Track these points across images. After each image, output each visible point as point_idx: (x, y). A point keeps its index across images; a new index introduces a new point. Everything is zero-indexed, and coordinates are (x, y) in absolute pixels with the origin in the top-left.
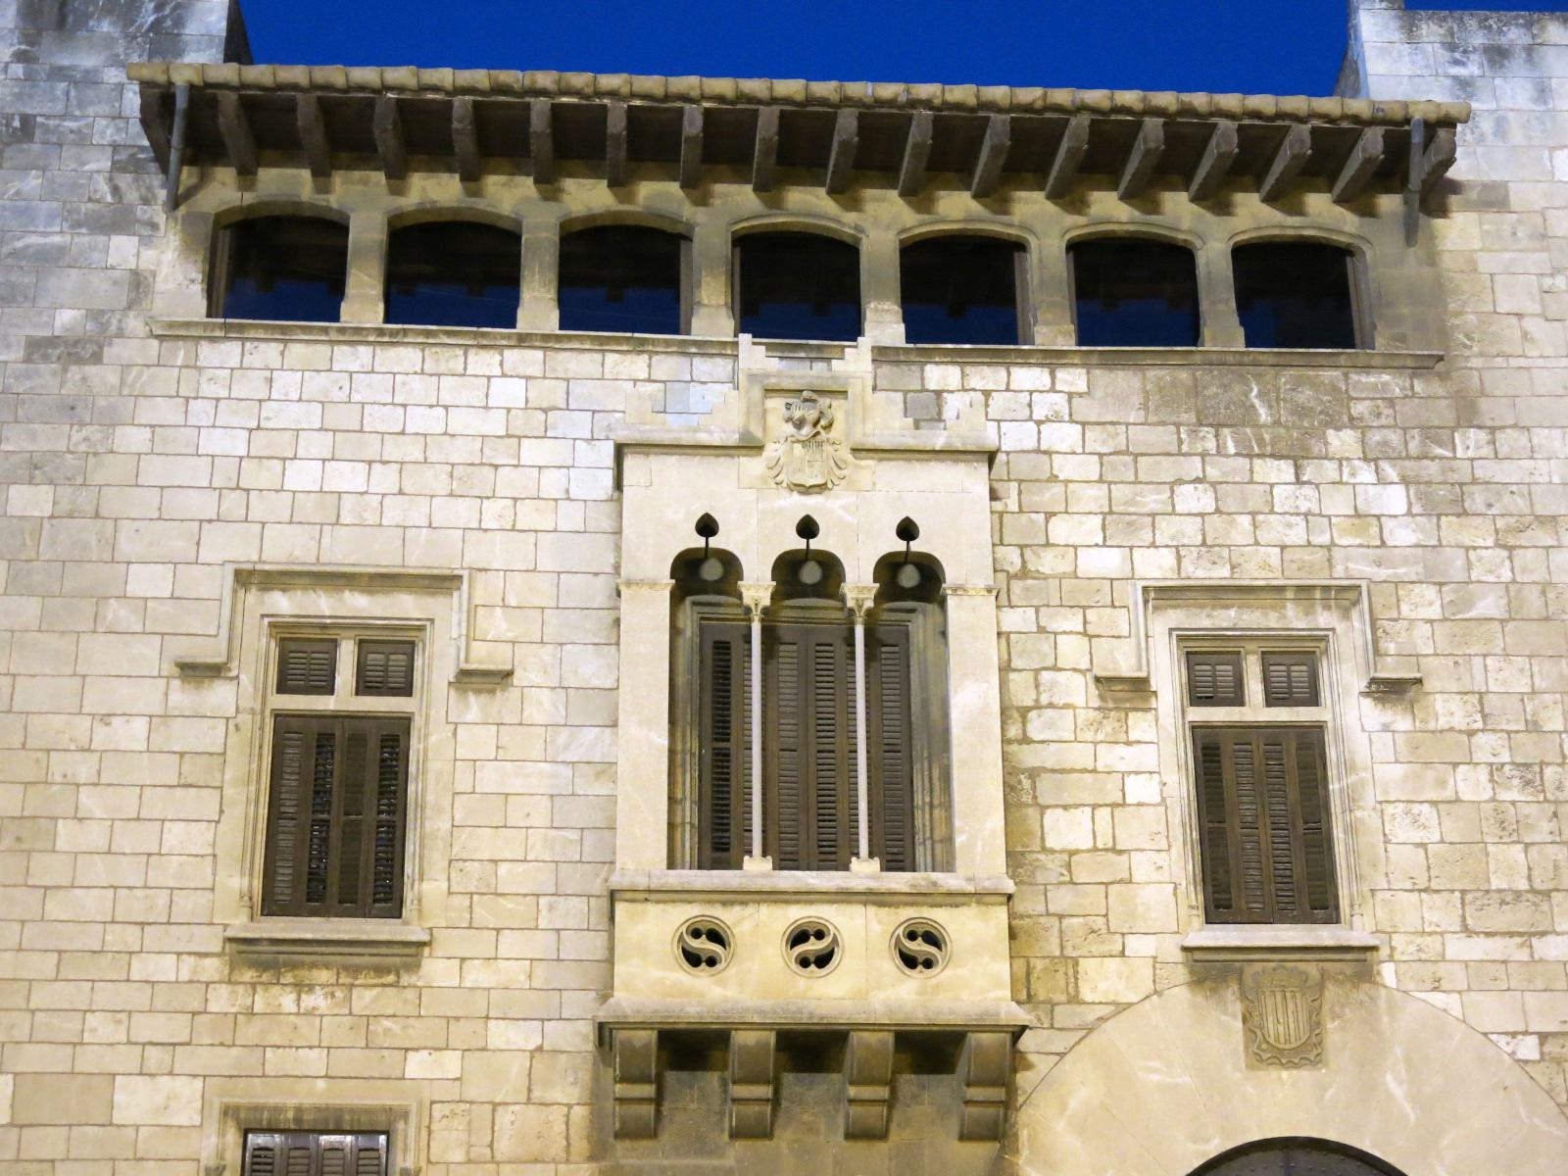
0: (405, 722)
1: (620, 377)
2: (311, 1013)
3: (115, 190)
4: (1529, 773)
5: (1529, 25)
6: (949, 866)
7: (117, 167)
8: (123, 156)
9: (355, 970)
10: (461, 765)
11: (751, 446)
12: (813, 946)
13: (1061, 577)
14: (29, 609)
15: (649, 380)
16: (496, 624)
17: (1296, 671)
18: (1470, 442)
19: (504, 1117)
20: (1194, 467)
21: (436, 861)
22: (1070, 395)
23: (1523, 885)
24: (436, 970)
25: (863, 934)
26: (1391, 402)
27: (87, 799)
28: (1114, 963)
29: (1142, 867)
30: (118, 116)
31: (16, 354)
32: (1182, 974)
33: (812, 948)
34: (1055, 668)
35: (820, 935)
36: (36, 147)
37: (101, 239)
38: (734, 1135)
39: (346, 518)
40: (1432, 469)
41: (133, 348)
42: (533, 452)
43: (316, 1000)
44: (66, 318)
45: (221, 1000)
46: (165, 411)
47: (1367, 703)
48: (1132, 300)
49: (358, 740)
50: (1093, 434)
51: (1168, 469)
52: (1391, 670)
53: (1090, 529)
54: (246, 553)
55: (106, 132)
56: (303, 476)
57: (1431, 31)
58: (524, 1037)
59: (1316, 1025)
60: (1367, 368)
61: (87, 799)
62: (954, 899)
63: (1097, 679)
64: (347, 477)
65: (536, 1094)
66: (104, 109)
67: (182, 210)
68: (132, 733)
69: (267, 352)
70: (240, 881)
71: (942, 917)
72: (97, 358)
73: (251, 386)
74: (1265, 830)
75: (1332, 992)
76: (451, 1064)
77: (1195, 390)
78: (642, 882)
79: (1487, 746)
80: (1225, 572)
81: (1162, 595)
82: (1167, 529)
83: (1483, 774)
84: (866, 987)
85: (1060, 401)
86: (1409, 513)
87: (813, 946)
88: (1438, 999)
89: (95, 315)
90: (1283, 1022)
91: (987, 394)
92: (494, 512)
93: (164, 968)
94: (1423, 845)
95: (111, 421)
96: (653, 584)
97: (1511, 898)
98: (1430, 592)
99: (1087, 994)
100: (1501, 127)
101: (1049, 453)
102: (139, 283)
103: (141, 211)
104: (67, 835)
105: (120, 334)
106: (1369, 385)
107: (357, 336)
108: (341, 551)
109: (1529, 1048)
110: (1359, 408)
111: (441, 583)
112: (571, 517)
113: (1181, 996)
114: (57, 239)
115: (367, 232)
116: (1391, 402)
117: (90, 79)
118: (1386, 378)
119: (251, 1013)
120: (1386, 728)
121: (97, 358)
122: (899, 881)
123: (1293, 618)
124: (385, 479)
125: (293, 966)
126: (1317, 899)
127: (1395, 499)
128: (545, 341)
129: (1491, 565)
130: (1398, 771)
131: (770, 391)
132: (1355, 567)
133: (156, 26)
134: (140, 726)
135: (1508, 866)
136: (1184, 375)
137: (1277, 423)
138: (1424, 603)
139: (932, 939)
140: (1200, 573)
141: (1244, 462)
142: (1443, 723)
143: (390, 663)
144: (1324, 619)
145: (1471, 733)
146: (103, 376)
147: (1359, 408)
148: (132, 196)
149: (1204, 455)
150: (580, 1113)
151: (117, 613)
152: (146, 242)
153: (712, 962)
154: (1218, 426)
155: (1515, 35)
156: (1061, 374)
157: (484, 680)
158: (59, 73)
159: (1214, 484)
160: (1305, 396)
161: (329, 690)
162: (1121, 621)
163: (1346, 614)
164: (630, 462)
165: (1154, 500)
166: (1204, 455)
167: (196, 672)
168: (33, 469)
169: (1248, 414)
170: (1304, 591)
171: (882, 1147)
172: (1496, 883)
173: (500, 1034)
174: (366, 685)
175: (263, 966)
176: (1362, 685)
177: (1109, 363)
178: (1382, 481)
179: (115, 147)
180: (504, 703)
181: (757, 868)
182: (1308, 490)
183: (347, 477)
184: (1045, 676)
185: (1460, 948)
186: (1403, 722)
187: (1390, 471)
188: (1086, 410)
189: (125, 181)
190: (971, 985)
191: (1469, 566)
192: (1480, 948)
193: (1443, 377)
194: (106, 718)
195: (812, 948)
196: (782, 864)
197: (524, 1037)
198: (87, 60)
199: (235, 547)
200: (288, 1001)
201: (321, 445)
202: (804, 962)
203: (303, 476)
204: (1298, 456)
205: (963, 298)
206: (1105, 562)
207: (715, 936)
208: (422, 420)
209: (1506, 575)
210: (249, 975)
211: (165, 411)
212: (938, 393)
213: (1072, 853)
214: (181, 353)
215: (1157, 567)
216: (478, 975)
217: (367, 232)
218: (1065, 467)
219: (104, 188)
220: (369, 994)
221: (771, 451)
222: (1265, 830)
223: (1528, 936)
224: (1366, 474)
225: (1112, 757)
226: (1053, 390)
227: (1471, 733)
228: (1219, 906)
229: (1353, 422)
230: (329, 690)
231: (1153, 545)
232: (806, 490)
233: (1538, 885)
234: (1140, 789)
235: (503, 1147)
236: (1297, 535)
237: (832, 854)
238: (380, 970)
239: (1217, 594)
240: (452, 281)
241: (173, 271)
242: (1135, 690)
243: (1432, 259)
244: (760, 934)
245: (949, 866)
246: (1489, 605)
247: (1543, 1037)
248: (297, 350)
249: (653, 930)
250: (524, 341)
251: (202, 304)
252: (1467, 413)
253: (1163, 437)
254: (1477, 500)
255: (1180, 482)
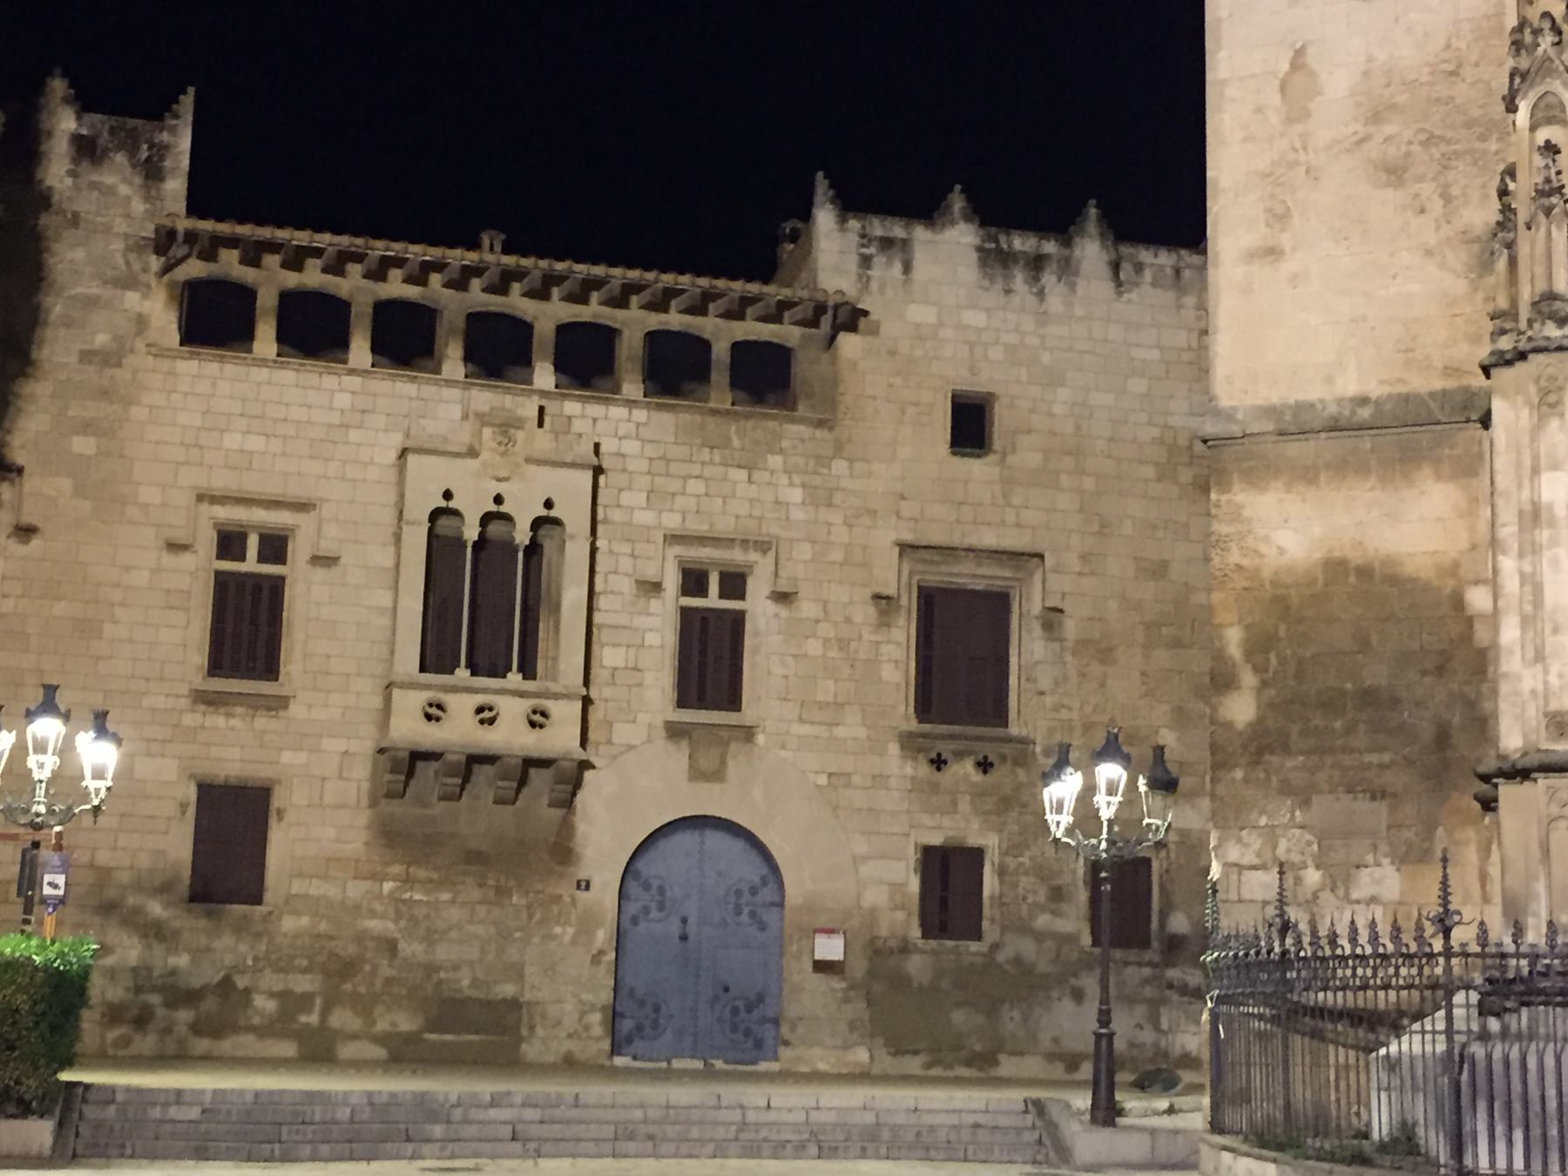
0: (282, 579)
1: (399, 391)
2: (233, 729)
3: (128, 263)
4: (843, 644)
5: (907, 226)
6: (555, 680)
7: (129, 249)
8: (131, 242)
9: (256, 708)
10: (308, 599)
11: (472, 453)
12: (487, 714)
13: (623, 524)
14: (86, 506)
15: (418, 398)
16: (331, 531)
17: (734, 584)
18: (840, 466)
19: (328, 785)
20: (696, 469)
21: (297, 654)
22: (638, 425)
23: (831, 699)
24: (295, 710)
25: (512, 710)
26: (803, 441)
27: (118, 611)
28: (629, 726)
29: (649, 678)
30: (128, 216)
31: (74, 359)
32: (663, 733)
33: (486, 715)
34: (615, 573)
35: (491, 709)
36: (80, 232)
37: (119, 292)
38: (442, 798)
39: (255, 465)
40: (817, 480)
41: (139, 359)
42: (355, 435)
43: (232, 722)
44: (101, 339)
45: (189, 719)
46: (158, 399)
47: (769, 602)
48: (674, 370)
49: (258, 588)
50: (648, 447)
51: (684, 469)
52: (783, 586)
53: (641, 498)
54: (202, 482)
55: (121, 226)
56: (232, 441)
57: (854, 224)
58: (339, 745)
59: (723, 763)
60: (793, 421)
61: (118, 611)
62: (557, 696)
63: (637, 581)
64: (256, 443)
65: (345, 774)
66: (120, 211)
67: (166, 278)
68: (140, 578)
69: (213, 368)
70: (199, 657)
71: (551, 706)
72: (119, 365)
73: (203, 387)
74: (710, 663)
75: (733, 747)
76: (302, 757)
77: (702, 427)
78: (407, 679)
79: (825, 629)
80: (705, 527)
81: (673, 539)
82: (680, 502)
83: (820, 642)
84: (510, 735)
85: (632, 426)
86: (803, 503)
87: (487, 714)
88: (783, 753)
89: (116, 338)
90: (707, 761)
91: (595, 420)
92: (333, 468)
93: (161, 702)
94: (786, 677)
95: (128, 402)
96: (419, 524)
97: (822, 706)
98: (807, 546)
99: (615, 740)
100: (882, 290)
101: (623, 456)
102: (141, 322)
103: (142, 277)
104: (108, 630)
105: (132, 351)
106: (794, 432)
107: (263, 362)
108: (252, 484)
109: (822, 780)
110: (785, 444)
111: (302, 507)
112: (373, 473)
113: (661, 742)
114: (95, 291)
115: (267, 300)
116: (803, 441)
117: (110, 191)
118: (802, 428)
119: (202, 727)
120: (776, 615)
121: (119, 365)
122: (530, 686)
123: (737, 556)
124: (275, 446)
125: (226, 704)
126: (732, 701)
127: (796, 495)
128: (363, 373)
129: (841, 534)
130: (780, 637)
131: (483, 424)
132: (772, 529)
133: (148, 159)
134: (146, 574)
135: (826, 689)
136: (698, 418)
137: (743, 449)
138: (804, 551)
139: (544, 714)
140: (696, 527)
141: (722, 469)
142: (804, 615)
143: (275, 547)
144: (753, 556)
145: (817, 622)
146: (123, 374)
147: (785, 444)
148: (137, 267)
149: (703, 463)
150: (366, 786)
151: (132, 512)
152: (145, 296)
153: (438, 719)
154: (712, 448)
155: (898, 230)
156: (635, 411)
157: (324, 561)
158: (94, 185)
159: (707, 480)
160: (759, 434)
161: (242, 558)
162: (650, 550)
163: (765, 552)
164: (412, 459)
165: (675, 485)
166: (703, 463)
167: (175, 547)
168: (87, 427)
169: (725, 444)
170: (745, 542)
171: (510, 808)
172: (819, 698)
173: (327, 743)
174: (262, 559)
175: (210, 703)
176: (767, 592)
177: (660, 407)
178: (791, 484)
179: (126, 236)
180: (334, 572)
181: (462, 673)
182: (753, 487)
183: (256, 443)
184: (611, 577)
185: (800, 730)
186: (783, 612)
187: (797, 479)
188: (644, 433)
189: (132, 257)
190: (561, 738)
191: (829, 533)
192: (805, 730)
193: (831, 429)
194: (128, 569)
195: (486, 715)
196: (474, 674)
197: (339, 745)
198: (108, 178)
199: (193, 478)
200: (220, 721)
201: (241, 423)
202: (482, 722)
203: (232, 441)
204: (750, 468)
205: (586, 361)
206: (647, 518)
207: (440, 707)
208: (296, 413)
209: (846, 540)
210: (203, 707)
211: (158, 399)
212: (569, 418)
213: (615, 669)
214: (165, 364)
215: (672, 522)
216: (317, 714)
217: (267, 300)
218: (632, 465)
219: (120, 261)
220: (263, 720)
221: (485, 455)
222: (710, 663)
223: (831, 725)
224: (784, 480)
225: (639, 621)
226: (629, 420)
227: (817, 622)
228: (682, 703)
229: (781, 451)
230: (242, 558)
231: (672, 511)
232: (499, 480)
233: (839, 700)
234: (652, 639)
235: (328, 799)
236: (743, 512)
237: (499, 671)
238: (270, 709)
239: (702, 540)
240: (313, 331)
241: (161, 315)
242: (656, 587)
243: (834, 362)
244: (461, 706)
245: (555, 680)
246: (837, 555)
247: (830, 775)
248: (229, 368)
249: (409, 703)
250: (352, 372)
251: (177, 338)
252: (839, 449)
253: (683, 451)
254: (837, 498)
255: (690, 477)
